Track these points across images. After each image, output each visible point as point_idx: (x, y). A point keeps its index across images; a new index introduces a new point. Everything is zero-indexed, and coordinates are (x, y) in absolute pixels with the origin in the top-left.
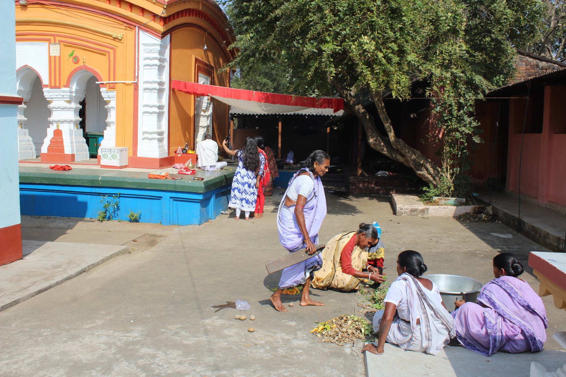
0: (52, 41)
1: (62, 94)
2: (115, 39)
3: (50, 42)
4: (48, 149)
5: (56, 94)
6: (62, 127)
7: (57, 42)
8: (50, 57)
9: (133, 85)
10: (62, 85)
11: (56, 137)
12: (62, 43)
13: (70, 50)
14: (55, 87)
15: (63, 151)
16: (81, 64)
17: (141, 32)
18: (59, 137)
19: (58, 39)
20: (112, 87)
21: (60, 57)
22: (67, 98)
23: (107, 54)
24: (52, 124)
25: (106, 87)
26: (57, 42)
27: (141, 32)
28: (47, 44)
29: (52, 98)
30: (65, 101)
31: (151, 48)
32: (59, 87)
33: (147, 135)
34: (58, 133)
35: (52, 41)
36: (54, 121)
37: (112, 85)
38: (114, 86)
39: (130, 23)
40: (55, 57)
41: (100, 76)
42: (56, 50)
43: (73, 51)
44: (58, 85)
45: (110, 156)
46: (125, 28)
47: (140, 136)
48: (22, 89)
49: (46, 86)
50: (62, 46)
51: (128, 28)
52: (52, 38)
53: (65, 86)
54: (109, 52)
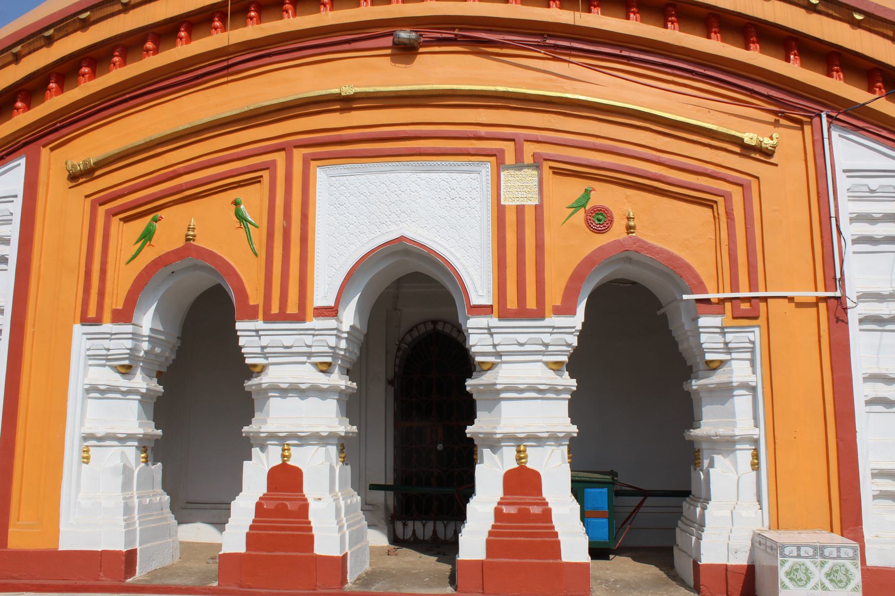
0: (510, 158)
1: (547, 338)
2: (747, 150)
3: (500, 164)
4: (489, 543)
5: (522, 338)
7: (528, 159)
8: (500, 211)
10: (548, 308)
11: (516, 498)
12: (546, 165)
13: (575, 188)
14: (522, 313)
15: (559, 556)
16: (617, 232)
17: (835, 134)
18: (529, 499)
19: (529, 149)
20: (747, 311)
22: (561, 353)
23: (720, 200)
25: (722, 313)
26: (528, 159)
27: (835, 134)
28: (486, 169)
29: (499, 355)
30: (546, 363)
31: (874, 183)
32: (539, 314)
34: (523, 482)
35: (510, 158)
36: (273, 436)
37: (745, 306)
39: (794, 105)
40: (520, 209)
41: (697, 277)
42: (521, 187)
43: (587, 192)
46: (771, 118)
47: (868, 487)
48: (359, 327)
49: (483, 310)
50: (547, 173)
51: (783, 121)
52: (508, 147)
54: (727, 196)
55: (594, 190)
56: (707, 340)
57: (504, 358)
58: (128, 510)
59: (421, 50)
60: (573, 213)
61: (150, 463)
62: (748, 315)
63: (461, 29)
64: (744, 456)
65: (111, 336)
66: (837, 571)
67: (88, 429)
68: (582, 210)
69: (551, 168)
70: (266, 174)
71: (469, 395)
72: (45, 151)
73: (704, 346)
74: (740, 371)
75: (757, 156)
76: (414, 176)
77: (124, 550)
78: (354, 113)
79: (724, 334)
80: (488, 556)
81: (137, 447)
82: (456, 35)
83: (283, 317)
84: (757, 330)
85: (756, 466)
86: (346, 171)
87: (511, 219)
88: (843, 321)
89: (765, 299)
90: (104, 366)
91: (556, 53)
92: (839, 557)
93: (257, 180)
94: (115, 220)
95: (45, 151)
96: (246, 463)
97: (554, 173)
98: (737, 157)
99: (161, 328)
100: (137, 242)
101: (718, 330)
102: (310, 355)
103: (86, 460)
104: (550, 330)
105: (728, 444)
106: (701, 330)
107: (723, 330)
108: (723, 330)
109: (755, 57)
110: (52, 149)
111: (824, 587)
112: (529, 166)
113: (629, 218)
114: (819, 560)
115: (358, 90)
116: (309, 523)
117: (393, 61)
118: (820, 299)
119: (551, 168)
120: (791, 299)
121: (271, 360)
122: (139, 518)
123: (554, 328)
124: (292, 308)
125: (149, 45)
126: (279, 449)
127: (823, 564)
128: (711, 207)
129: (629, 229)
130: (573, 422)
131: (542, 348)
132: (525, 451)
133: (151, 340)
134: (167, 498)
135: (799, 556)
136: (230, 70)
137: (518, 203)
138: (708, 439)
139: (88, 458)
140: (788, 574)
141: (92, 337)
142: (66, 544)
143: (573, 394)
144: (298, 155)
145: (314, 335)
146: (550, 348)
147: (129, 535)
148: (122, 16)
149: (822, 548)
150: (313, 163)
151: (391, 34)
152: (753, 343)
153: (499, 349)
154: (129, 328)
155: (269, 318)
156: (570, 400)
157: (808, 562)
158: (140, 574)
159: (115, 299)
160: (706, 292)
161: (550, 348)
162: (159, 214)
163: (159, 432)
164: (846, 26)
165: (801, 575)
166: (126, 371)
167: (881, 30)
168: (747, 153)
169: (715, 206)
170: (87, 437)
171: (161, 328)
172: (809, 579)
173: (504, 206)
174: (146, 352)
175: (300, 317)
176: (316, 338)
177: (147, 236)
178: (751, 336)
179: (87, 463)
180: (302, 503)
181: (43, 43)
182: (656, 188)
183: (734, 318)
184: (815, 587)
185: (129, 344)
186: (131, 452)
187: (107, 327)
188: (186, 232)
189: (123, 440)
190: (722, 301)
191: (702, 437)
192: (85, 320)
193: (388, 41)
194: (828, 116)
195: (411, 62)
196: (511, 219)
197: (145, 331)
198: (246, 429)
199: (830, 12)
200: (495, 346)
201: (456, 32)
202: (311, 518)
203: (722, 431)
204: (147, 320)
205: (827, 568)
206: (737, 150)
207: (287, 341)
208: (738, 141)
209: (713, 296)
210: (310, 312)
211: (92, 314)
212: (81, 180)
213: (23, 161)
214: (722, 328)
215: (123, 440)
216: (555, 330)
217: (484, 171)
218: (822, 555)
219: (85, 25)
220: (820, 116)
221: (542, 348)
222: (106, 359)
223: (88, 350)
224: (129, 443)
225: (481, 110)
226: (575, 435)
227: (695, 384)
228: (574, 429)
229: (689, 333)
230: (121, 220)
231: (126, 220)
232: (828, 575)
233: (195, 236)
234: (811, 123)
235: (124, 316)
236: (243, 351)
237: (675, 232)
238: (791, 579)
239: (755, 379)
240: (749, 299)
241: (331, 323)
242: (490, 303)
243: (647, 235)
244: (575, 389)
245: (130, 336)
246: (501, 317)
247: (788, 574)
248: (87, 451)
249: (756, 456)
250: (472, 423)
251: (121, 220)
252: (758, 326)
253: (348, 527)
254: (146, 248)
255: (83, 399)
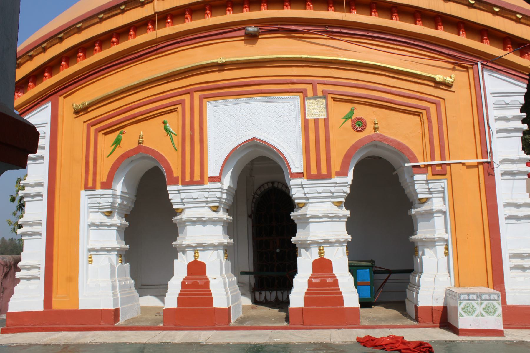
0: (310, 94)
1: (333, 189)
2: (438, 84)
3: (305, 97)
4: (305, 298)
5: (320, 190)
6: (204, 257)
7: (320, 94)
8: (306, 122)
9: (481, 167)
10: (333, 173)
11: (319, 274)
12: (330, 96)
13: (346, 108)
14: (319, 176)
15: (343, 304)
16: (369, 131)
17: (486, 74)
18: (326, 275)
19: (320, 88)
20: (440, 171)
21: (326, 120)
22: (341, 197)
23: (424, 112)
24: (184, 252)
25: (426, 172)
26: (320, 94)
28: (297, 99)
29: (308, 199)
30: (333, 203)
31: (508, 100)
32: (328, 176)
33: (518, 262)
34: (322, 266)
35: (310, 94)
37: (439, 168)
38: (444, 170)
39: (463, 59)
40: (316, 121)
41: (412, 154)
42: (316, 109)
43: (352, 110)
44: (324, 171)
45: (479, 309)
46: (451, 66)
48: (232, 186)
50: (330, 101)
51: (457, 68)
52: (309, 88)
53: (338, 175)
54: (427, 110)
55: (355, 109)
56: (419, 187)
57: (311, 201)
58: (114, 287)
59: (260, 37)
60: (345, 122)
61: (123, 263)
62: (442, 173)
63: (281, 25)
64: (440, 249)
65: (101, 196)
66: (489, 307)
67: (91, 246)
68: (349, 121)
69: (332, 98)
70: (180, 107)
71: (293, 221)
72: (61, 99)
73: (417, 191)
74: (437, 203)
75: (444, 87)
76: (259, 105)
77: (113, 308)
78: (226, 72)
79: (428, 184)
80: (305, 305)
81: (117, 255)
82: (279, 28)
83: (192, 182)
84: (445, 181)
85: (447, 254)
86: (222, 104)
87: (312, 126)
88: (492, 175)
89: (449, 164)
90: (98, 212)
91: (332, 35)
92: (490, 299)
93: (175, 110)
94: (100, 134)
95: (61, 99)
96: (175, 261)
97: (334, 100)
98: (432, 88)
99: (126, 191)
100: (113, 145)
101: (425, 182)
102: (207, 202)
103: (91, 262)
104: (335, 185)
105: (431, 243)
106: (415, 182)
107: (427, 182)
108: (427, 182)
109: (441, 33)
110: (65, 98)
111: (482, 316)
112: (320, 97)
113: (375, 124)
114: (479, 301)
115: (227, 60)
116: (210, 291)
117: (245, 43)
118: (479, 163)
119: (332, 98)
120: (463, 164)
121: (187, 206)
122: (120, 292)
123: (336, 183)
124: (197, 178)
125: (114, 39)
126: (193, 252)
127: (481, 303)
128: (419, 116)
129: (375, 129)
130: (348, 234)
131: (331, 195)
132: (323, 249)
133: (122, 197)
134: (133, 281)
135: (469, 299)
136: (158, 51)
137: (315, 118)
138: (421, 240)
139: (91, 261)
140: (463, 309)
141: (90, 197)
142: (81, 308)
143: (348, 218)
144: (196, 95)
145: (209, 192)
146: (335, 194)
147: (115, 300)
148: (99, 24)
149: (481, 295)
150: (204, 100)
151: (244, 29)
152: (444, 188)
153: (308, 195)
154: (110, 192)
155: (184, 184)
156: (346, 222)
157: (473, 303)
158: (122, 321)
159: (102, 177)
160: (418, 162)
161: (335, 194)
162: (123, 130)
163: (128, 246)
164: (490, 15)
165: (470, 309)
166: (109, 214)
167: (509, 16)
168: (438, 86)
169: (421, 115)
170: (90, 250)
171: (126, 191)
172: (474, 311)
173: (308, 119)
174: (119, 204)
175: (201, 182)
176: (210, 193)
177: (118, 142)
178: (443, 185)
179: (91, 264)
180: (206, 280)
181: (58, 41)
182: (389, 107)
183: (433, 175)
184: (477, 316)
185: (111, 200)
186: (114, 257)
187: (99, 191)
188: (138, 139)
189: (109, 251)
190: (426, 166)
191: (418, 239)
192: (87, 188)
193: (242, 33)
194: (482, 64)
195: (254, 43)
196: (312, 126)
197: (119, 192)
198: (174, 243)
199: (481, 7)
200: (305, 194)
201: (279, 26)
202: (211, 288)
203: (428, 236)
204: (119, 187)
205: (483, 305)
206: (433, 84)
207: (195, 195)
208: (433, 80)
209: (421, 164)
210: (206, 179)
211: (90, 184)
212: (81, 114)
213: (49, 105)
214: (427, 181)
215: (109, 251)
216: (337, 185)
217: (296, 101)
218: (481, 299)
219: (79, 30)
220: (477, 64)
221: (331, 195)
222: (98, 208)
223: (89, 204)
224: (112, 253)
225: (294, 68)
226: (350, 240)
227: (413, 211)
228: (349, 237)
229: (409, 184)
230: (103, 134)
231: (106, 134)
232: (484, 309)
233: (143, 141)
234: (472, 68)
235: (107, 185)
236: (171, 201)
237: (400, 130)
238: (465, 312)
239: (445, 207)
240: (441, 165)
241: (218, 185)
242: (302, 171)
243: (386, 132)
244: (349, 216)
245: (111, 196)
246: (308, 179)
247: (463, 309)
248: (91, 258)
249: (447, 248)
250: (295, 236)
251: (103, 134)
252: (446, 179)
253: (231, 293)
254: (117, 149)
255: (88, 229)
